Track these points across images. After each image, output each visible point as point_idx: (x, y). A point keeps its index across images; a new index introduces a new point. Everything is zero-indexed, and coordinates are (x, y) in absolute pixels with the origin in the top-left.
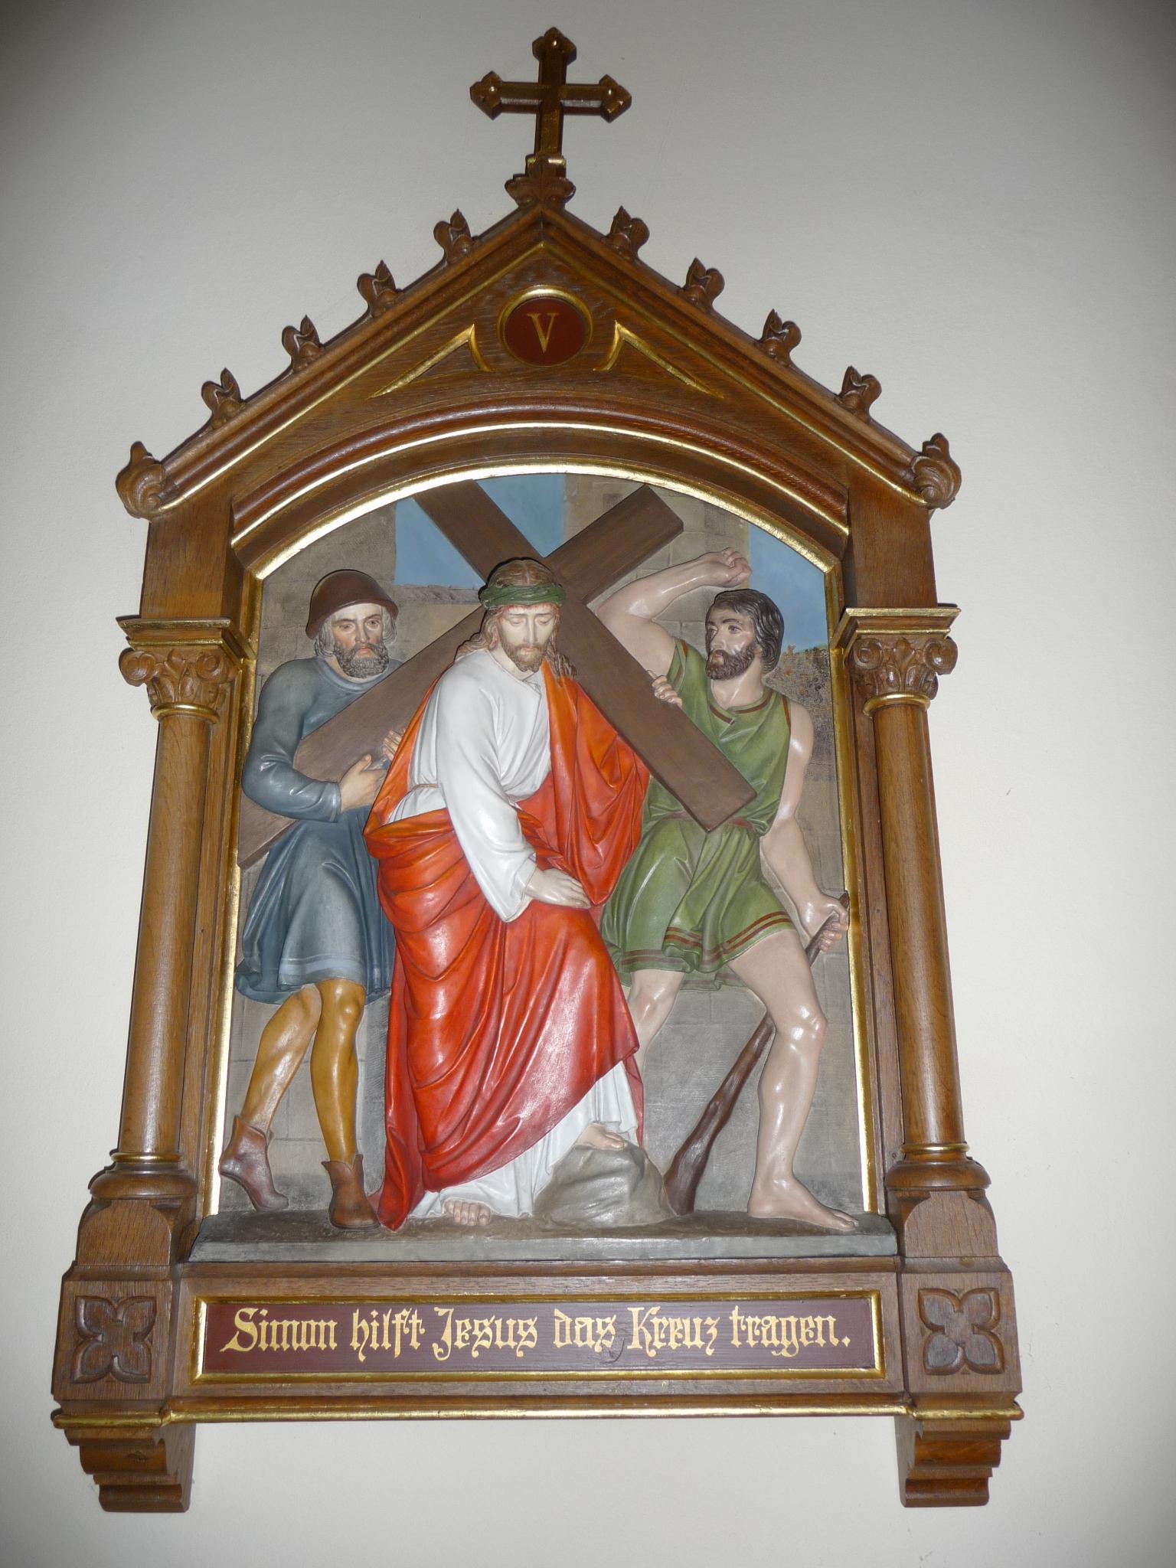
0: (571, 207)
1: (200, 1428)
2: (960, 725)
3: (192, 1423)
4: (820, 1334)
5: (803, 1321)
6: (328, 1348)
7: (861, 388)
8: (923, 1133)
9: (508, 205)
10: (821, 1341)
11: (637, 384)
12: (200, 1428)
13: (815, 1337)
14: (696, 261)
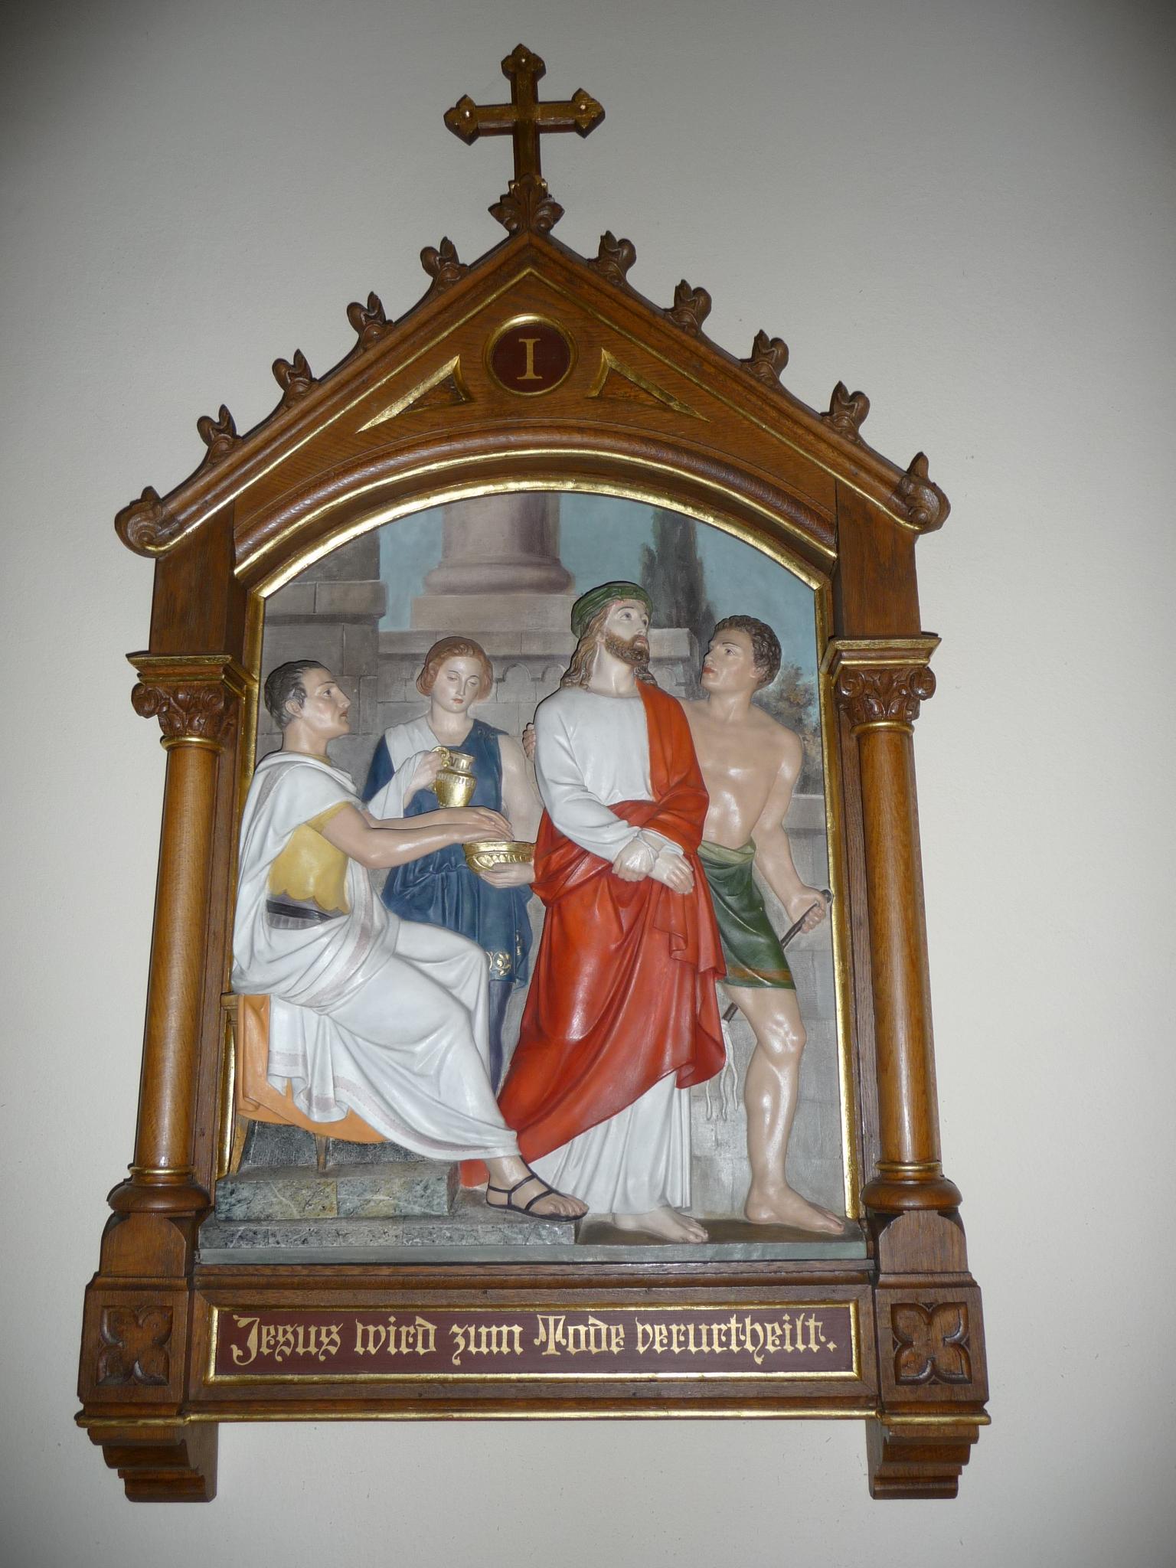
0: (559, 232)
1: (222, 1426)
2: (942, 741)
3: (217, 1422)
4: (788, 1341)
5: (613, 1329)
6: (367, 1353)
7: (849, 405)
8: (899, 1146)
9: (499, 233)
10: (789, 1348)
11: (613, 408)
12: (222, 1426)
13: (782, 1343)
14: (683, 282)
